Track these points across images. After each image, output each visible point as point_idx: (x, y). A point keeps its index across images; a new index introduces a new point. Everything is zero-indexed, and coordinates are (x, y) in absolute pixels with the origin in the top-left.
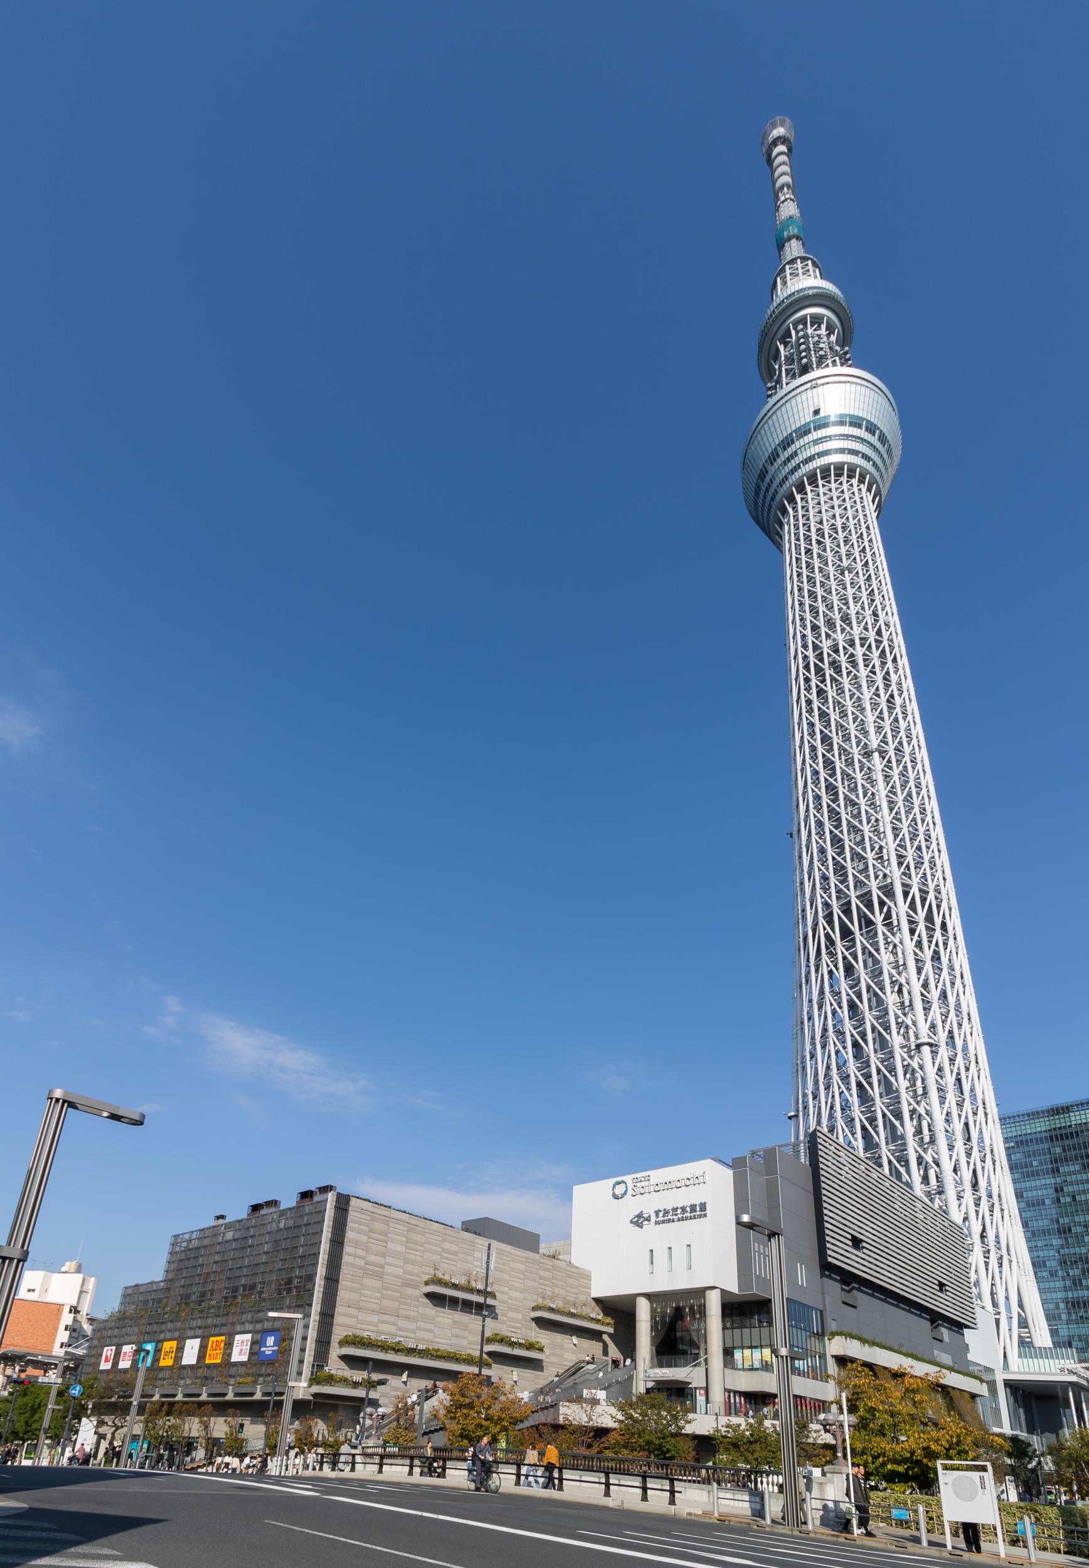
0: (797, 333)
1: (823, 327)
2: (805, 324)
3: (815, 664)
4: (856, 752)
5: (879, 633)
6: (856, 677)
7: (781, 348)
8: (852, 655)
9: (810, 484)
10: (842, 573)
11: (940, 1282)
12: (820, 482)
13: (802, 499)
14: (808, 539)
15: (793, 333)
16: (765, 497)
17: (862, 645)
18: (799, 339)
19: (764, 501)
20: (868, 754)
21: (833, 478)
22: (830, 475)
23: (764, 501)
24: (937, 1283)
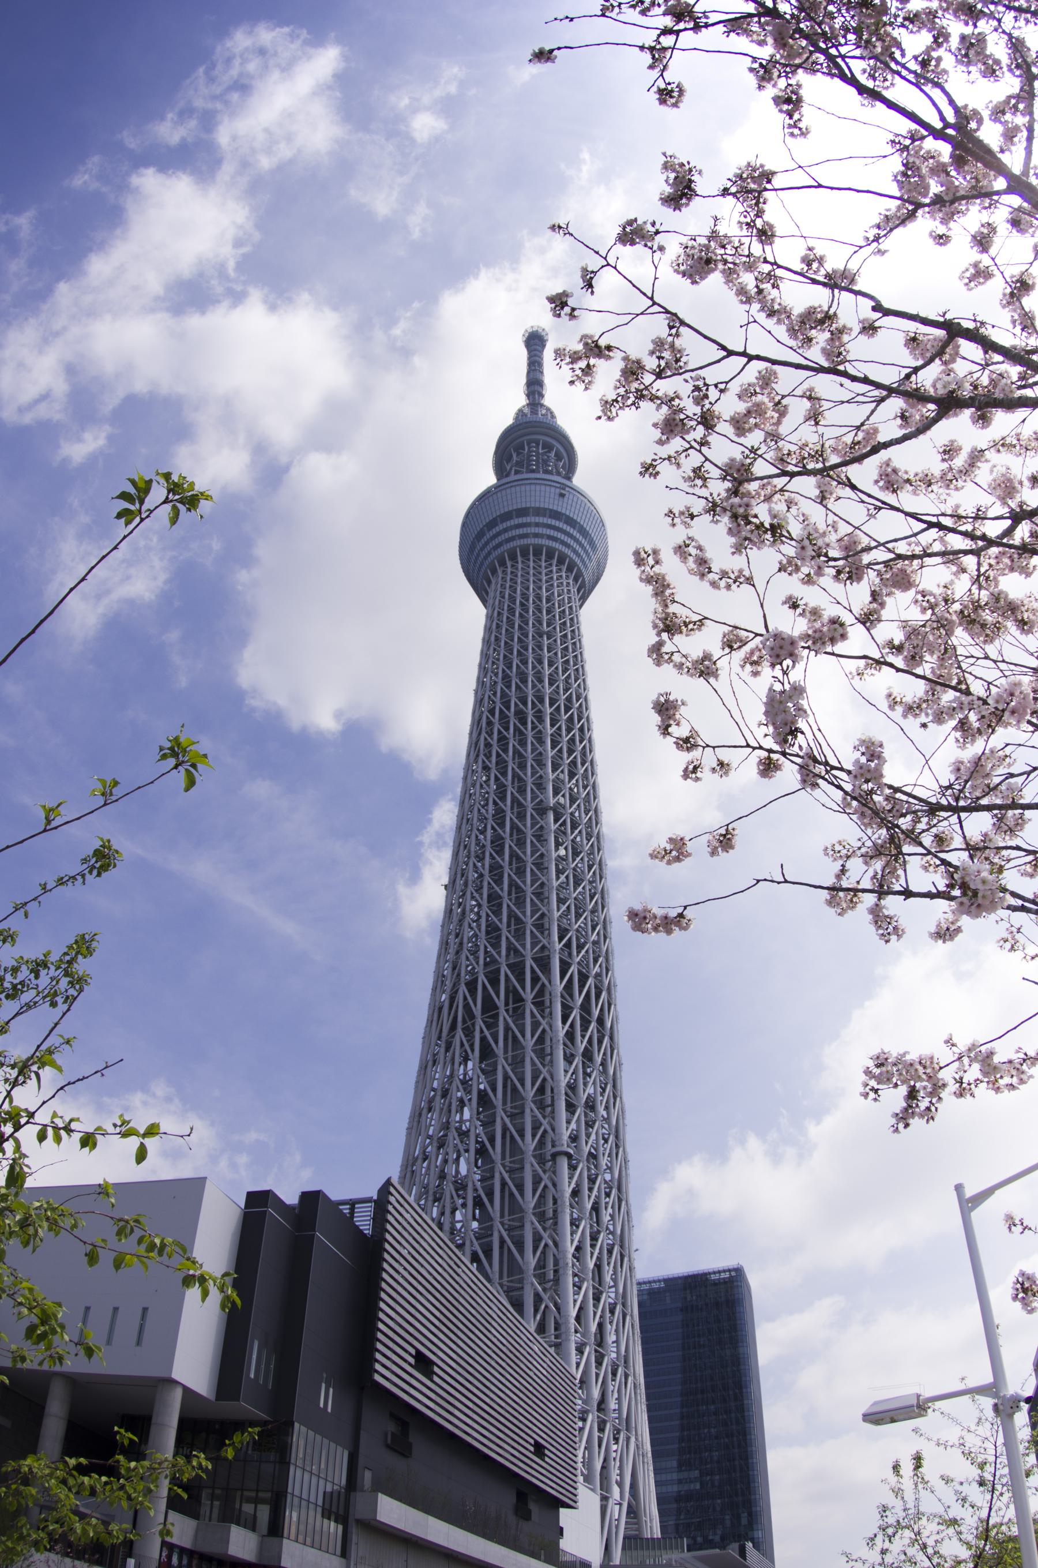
0: (529, 448)
1: (552, 454)
2: (538, 444)
3: (501, 710)
4: (529, 806)
5: (569, 699)
6: (540, 732)
7: (514, 455)
8: (540, 711)
9: (522, 556)
10: (541, 636)
11: (536, 1442)
12: (531, 557)
13: (512, 566)
14: (512, 599)
15: (526, 448)
16: (478, 555)
17: (551, 705)
18: (530, 451)
19: (476, 559)
20: (541, 810)
21: (543, 558)
22: (541, 554)
23: (476, 559)
24: (532, 1442)
